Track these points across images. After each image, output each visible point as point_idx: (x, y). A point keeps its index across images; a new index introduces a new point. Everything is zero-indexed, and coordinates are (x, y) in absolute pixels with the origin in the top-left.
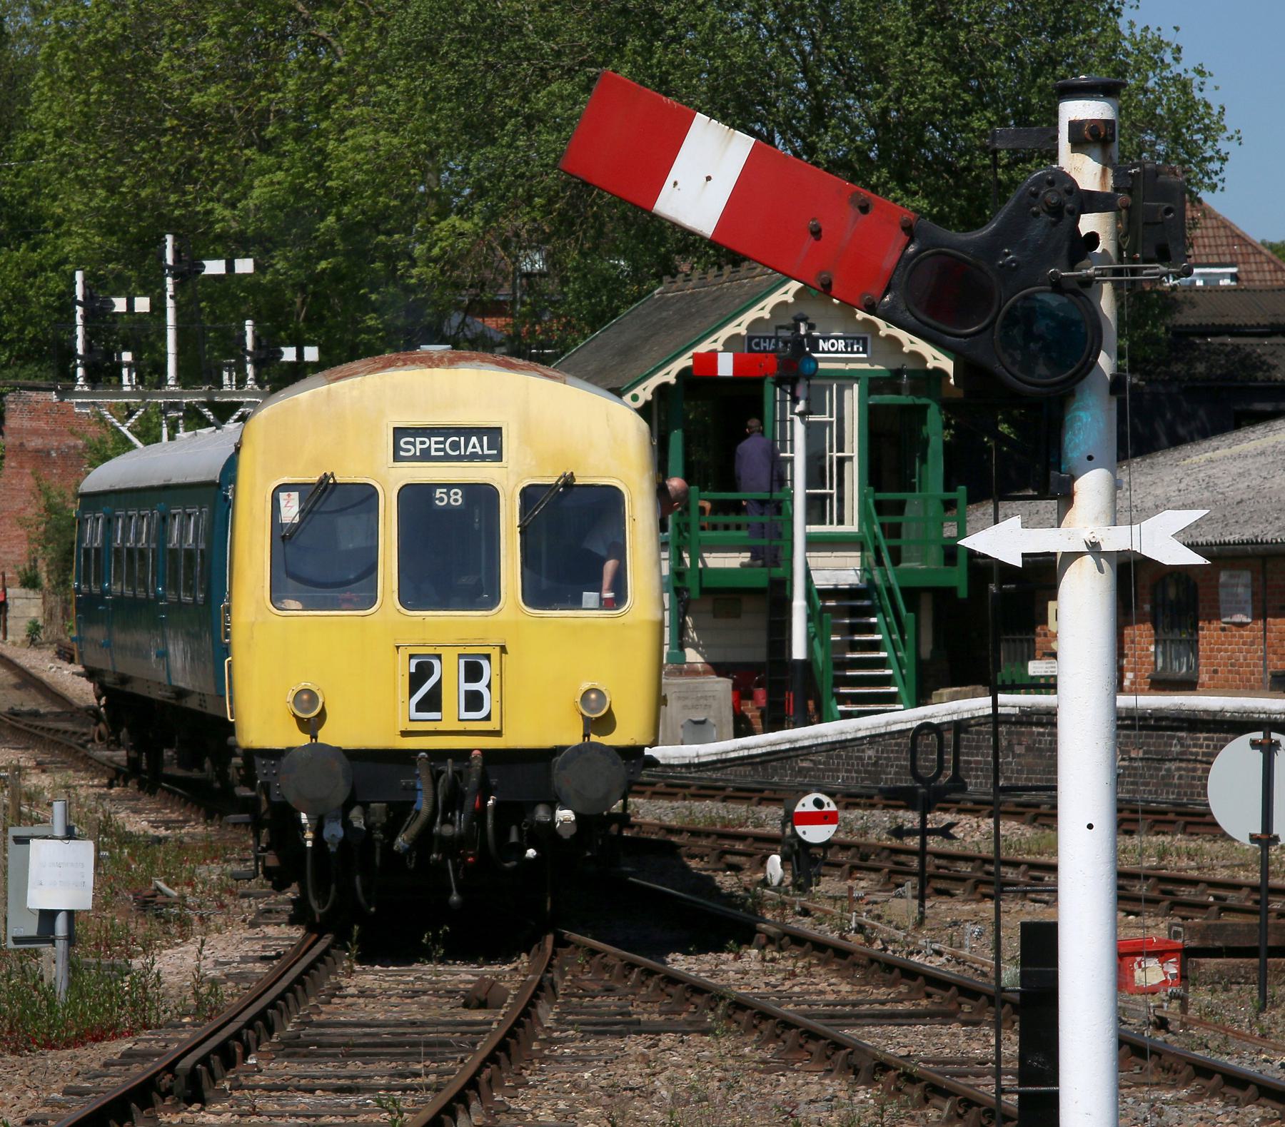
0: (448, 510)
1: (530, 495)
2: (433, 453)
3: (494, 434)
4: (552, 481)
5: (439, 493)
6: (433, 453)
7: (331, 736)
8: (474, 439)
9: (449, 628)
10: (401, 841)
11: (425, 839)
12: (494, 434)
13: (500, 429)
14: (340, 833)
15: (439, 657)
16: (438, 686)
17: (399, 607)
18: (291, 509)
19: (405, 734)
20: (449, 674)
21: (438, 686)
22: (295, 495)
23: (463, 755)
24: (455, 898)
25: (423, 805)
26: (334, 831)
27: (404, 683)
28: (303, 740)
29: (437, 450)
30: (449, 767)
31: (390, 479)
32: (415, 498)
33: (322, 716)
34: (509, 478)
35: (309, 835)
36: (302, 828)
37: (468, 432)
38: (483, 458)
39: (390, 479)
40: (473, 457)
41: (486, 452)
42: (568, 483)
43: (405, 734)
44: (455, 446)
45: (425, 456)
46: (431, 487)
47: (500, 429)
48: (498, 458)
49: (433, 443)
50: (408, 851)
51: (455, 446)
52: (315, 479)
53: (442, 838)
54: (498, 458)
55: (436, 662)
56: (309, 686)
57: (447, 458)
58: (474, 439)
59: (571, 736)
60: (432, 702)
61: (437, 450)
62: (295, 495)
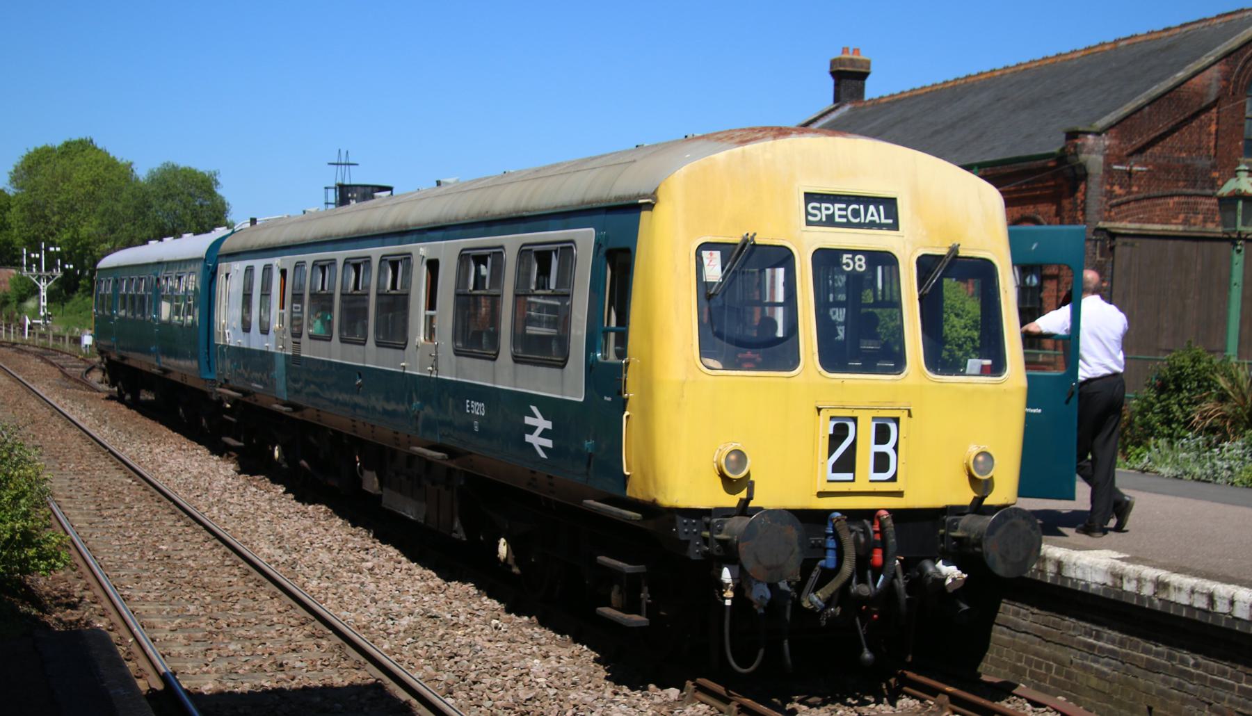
1: (926, 265)
2: (837, 220)
3: (890, 204)
5: (846, 258)
6: (837, 220)
8: (872, 208)
9: (863, 391)
12: (890, 204)
13: (895, 199)
14: (768, 595)
15: (855, 420)
17: (820, 369)
18: (714, 270)
19: (821, 494)
22: (717, 254)
23: (871, 514)
26: (760, 593)
27: (824, 444)
29: (840, 216)
31: (805, 242)
32: (826, 260)
34: (907, 245)
35: (729, 594)
36: (721, 586)
37: (867, 200)
38: (880, 226)
39: (805, 242)
40: (872, 225)
41: (884, 221)
43: (821, 494)
44: (856, 213)
45: (830, 221)
47: (895, 199)
48: (895, 226)
51: (856, 213)
54: (895, 226)
55: (851, 425)
56: (739, 446)
57: (849, 225)
58: (872, 208)
59: (965, 496)
60: (846, 464)
61: (840, 216)
62: (717, 254)
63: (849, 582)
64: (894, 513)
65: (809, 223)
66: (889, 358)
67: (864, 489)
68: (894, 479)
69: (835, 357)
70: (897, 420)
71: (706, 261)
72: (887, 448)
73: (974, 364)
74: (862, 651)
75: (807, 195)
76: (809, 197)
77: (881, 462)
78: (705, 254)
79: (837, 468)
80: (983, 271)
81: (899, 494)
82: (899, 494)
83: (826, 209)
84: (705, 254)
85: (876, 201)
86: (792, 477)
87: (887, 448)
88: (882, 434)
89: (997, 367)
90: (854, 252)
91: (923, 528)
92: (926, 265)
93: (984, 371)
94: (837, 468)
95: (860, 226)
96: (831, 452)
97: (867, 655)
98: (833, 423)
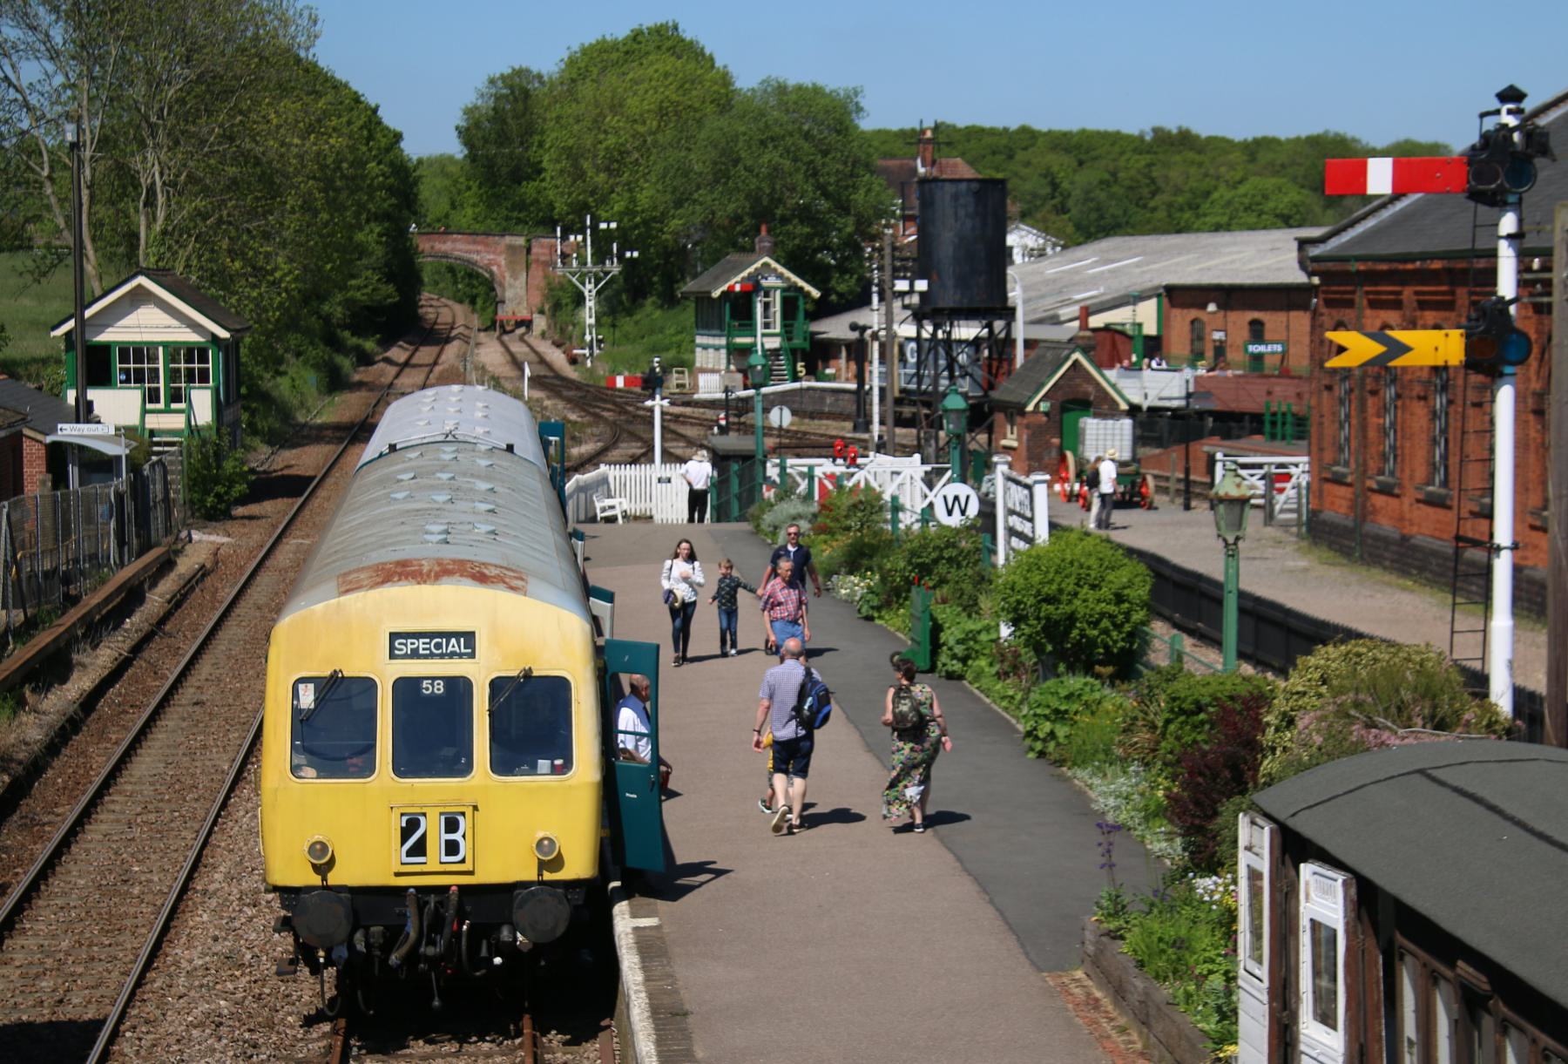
0: (433, 697)
1: (497, 685)
3: (469, 637)
4: (514, 674)
5: (425, 684)
7: (334, 878)
8: (453, 641)
9: (432, 793)
10: (394, 959)
11: (413, 957)
12: (469, 637)
14: (345, 954)
16: (423, 837)
18: (307, 698)
19: (397, 874)
20: (432, 828)
21: (423, 837)
22: (311, 686)
23: (444, 889)
24: (436, 1003)
25: (412, 930)
28: (316, 880)
30: (432, 899)
31: (386, 673)
32: (406, 688)
33: (331, 863)
34: (480, 672)
37: (448, 635)
38: (461, 656)
39: (386, 673)
40: (452, 655)
42: (528, 675)
43: (397, 874)
45: (415, 654)
46: (417, 681)
48: (472, 655)
49: (421, 644)
50: (400, 966)
52: (327, 673)
53: (427, 959)
54: (472, 655)
55: (422, 819)
56: (321, 838)
57: (432, 656)
58: (453, 641)
59: (526, 871)
60: (419, 849)
62: (311, 686)
63: (418, 943)
64: (461, 888)
65: (392, 656)
66: (459, 765)
67: (435, 869)
68: (463, 861)
69: (403, 767)
70: (463, 814)
71: (301, 692)
72: (457, 836)
73: (544, 764)
74: (432, 999)
75: (394, 636)
76: (394, 636)
77: (452, 848)
78: (301, 687)
79: (410, 853)
80: (558, 688)
81: (471, 873)
82: (471, 873)
83: (411, 644)
84: (301, 687)
85: (457, 635)
86: (370, 861)
87: (457, 836)
88: (452, 825)
89: (567, 766)
90: (434, 679)
91: (494, 901)
92: (497, 685)
93: (555, 770)
94: (410, 853)
95: (442, 656)
96: (403, 843)
97: (436, 1003)
98: (405, 819)
